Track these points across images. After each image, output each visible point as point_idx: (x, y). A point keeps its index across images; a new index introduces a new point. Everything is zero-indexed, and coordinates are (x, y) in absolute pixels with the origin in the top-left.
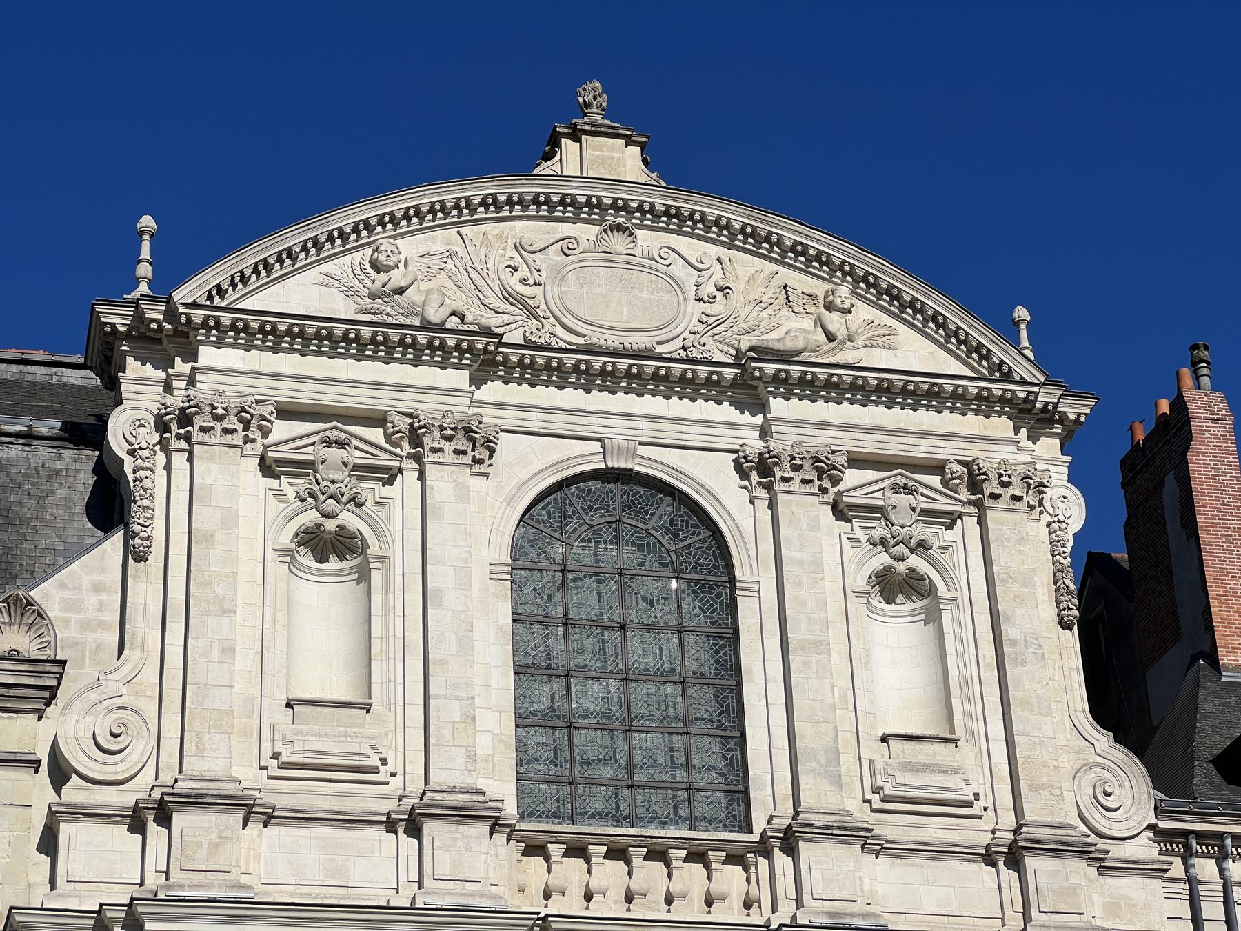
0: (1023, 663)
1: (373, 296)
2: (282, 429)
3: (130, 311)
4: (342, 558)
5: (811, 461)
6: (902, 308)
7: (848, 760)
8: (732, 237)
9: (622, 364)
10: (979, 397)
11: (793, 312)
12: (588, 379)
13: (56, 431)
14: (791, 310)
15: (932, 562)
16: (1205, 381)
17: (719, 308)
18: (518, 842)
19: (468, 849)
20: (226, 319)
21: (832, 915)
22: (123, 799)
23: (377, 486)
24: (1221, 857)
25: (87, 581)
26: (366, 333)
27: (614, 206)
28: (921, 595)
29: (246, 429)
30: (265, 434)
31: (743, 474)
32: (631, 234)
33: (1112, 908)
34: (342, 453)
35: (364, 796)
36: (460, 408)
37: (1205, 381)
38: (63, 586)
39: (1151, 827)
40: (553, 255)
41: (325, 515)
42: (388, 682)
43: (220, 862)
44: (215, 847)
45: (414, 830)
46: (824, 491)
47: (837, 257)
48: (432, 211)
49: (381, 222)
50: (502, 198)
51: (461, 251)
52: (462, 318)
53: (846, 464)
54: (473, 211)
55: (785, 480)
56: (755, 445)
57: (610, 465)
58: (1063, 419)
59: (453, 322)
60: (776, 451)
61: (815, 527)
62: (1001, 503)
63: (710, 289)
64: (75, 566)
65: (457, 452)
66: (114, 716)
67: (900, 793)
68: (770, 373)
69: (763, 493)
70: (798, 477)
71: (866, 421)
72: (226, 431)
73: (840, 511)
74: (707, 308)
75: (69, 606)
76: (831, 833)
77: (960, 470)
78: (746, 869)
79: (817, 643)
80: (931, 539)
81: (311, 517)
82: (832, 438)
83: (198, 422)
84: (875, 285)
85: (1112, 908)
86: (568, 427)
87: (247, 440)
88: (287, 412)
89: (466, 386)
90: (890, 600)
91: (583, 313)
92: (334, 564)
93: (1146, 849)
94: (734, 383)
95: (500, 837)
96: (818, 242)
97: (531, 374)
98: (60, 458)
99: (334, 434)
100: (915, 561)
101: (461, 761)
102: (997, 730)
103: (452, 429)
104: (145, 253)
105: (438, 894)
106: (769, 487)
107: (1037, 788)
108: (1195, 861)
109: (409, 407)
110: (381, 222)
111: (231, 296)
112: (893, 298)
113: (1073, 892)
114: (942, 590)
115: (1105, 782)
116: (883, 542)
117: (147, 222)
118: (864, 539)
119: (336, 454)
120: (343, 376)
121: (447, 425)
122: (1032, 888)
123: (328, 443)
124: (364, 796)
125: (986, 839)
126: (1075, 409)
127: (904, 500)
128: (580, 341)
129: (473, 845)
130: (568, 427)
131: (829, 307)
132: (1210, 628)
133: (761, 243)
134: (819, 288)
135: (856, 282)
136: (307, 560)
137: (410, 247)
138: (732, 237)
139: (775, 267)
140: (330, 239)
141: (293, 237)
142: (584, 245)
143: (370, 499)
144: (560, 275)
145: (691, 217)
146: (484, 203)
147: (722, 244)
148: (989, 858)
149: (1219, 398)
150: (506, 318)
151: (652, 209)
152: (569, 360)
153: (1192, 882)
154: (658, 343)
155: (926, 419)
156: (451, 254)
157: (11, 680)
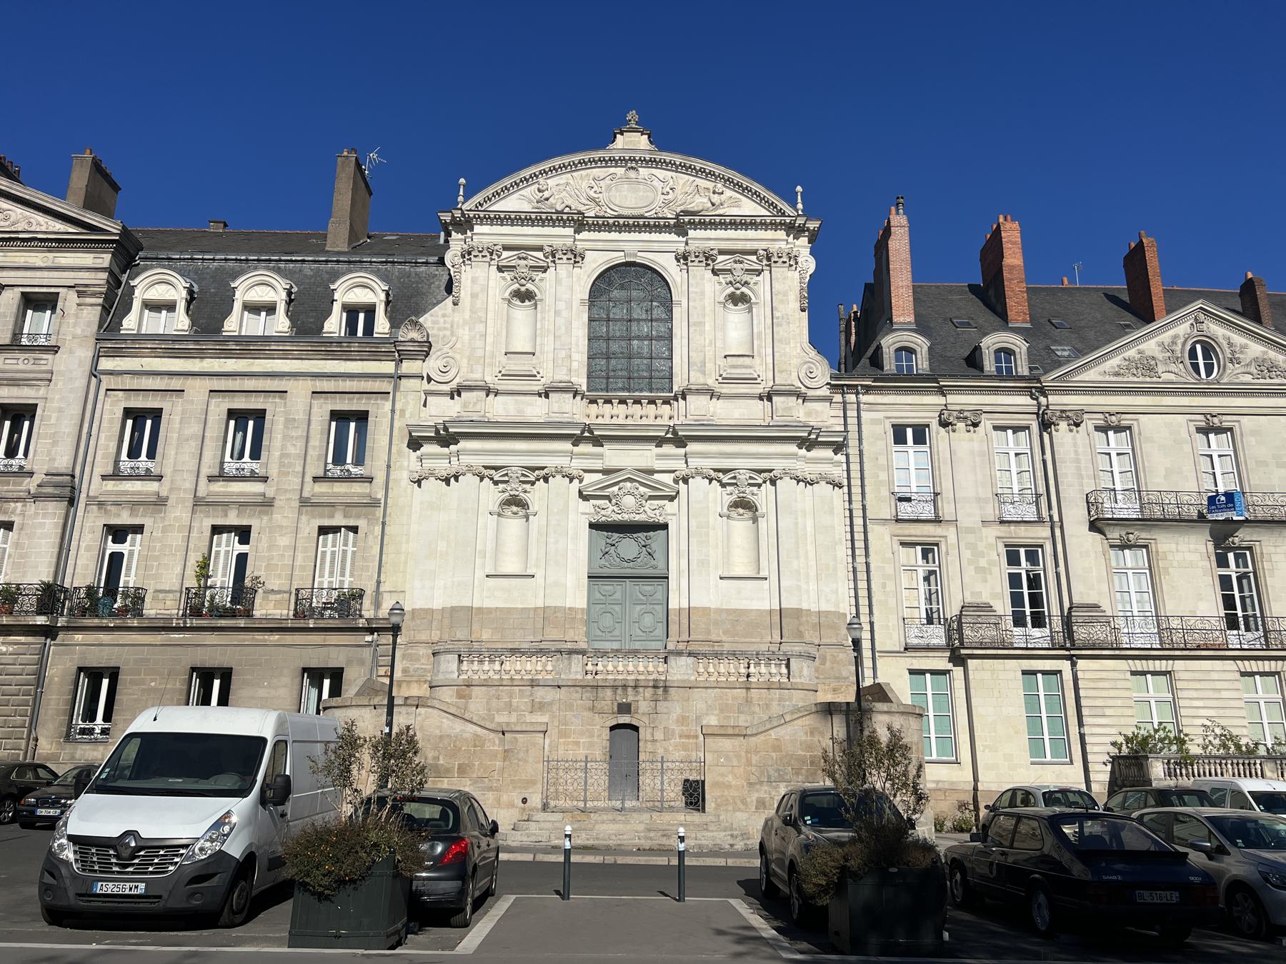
0: (781, 325)
1: (538, 202)
2: (505, 254)
3: (450, 214)
4: (530, 301)
6: (743, 190)
7: (709, 366)
8: (677, 168)
9: (631, 221)
10: (771, 223)
12: (620, 228)
13: (436, 261)
15: (750, 289)
16: (901, 211)
17: (670, 197)
19: (564, 402)
20: (482, 215)
21: (696, 421)
22: (446, 388)
24: (857, 394)
25: (440, 313)
26: (533, 216)
27: (630, 159)
28: (747, 302)
29: (575, 257)
30: (499, 257)
31: (678, 260)
33: (809, 414)
34: (525, 262)
35: (531, 385)
36: (569, 242)
37: (901, 211)
38: (432, 315)
39: (828, 384)
40: (607, 181)
42: (760, 346)
43: (477, 409)
44: (475, 404)
45: (770, 399)
46: (709, 265)
47: (717, 173)
48: (560, 167)
49: (541, 173)
50: (586, 160)
51: (572, 182)
52: (570, 208)
54: (576, 166)
55: (692, 261)
56: (681, 248)
58: (808, 230)
59: (567, 210)
61: (702, 279)
62: (778, 265)
63: (668, 189)
64: (436, 308)
65: (568, 259)
66: (445, 360)
67: (728, 376)
68: (686, 220)
69: (685, 267)
70: (697, 260)
71: (726, 237)
72: (483, 256)
73: (715, 272)
74: (666, 197)
75: (434, 322)
76: (699, 392)
77: (762, 252)
79: (700, 322)
80: (749, 280)
81: (516, 286)
82: (712, 244)
83: (473, 253)
84: (733, 182)
85: (809, 414)
87: (575, 262)
88: (506, 248)
89: (572, 234)
90: (736, 305)
91: (617, 203)
92: (527, 303)
93: (825, 392)
94: (675, 226)
95: (578, 398)
96: (710, 166)
97: (598, 227)
98: (437, 270)
99: (521, 255)
100: (744, 289)
101: (565, 371)
102: (770, 351)
104: (461, 193)
105: (778, 420)
107: (781, 372)
108: (847, 396)
109: (550, 243)
110: (541, 173)
111: (485, 206)
112: (740, 187)
113: (790, 408)
114: (754, 300)
115: (810, 368)
116: (731, 282)
117: (462, 181)
118: (724, 282)
119: (523, 262)
120: (527, 233)
122: (774, 408)
123: (520, 258)
124: (531, 385)
125: (761, 391)
126: (813, 225)
127: (738, 266)
128: (616, 214)
129: (567, 401)
131: (714, 192)
132: (891, 308)
133: (688, 169)
134: (710, 185)
135: (725, 181)
136: (731, 306)
137: (551, 182)
138: (677, 168)
140: (521, 181)
141: (507, 182)
142: (619, 176)
143: (537, 279)
144: (609, 188)
145: (660, 161)
146: (580, 162)
147: (673, 171)
148: (761, 398)
149: (905, 217)
150: (588, 207)
152: (611, 221)
153: (844, 403)
155: (751, 233)
156: (567, 184)
157: (412, 349)
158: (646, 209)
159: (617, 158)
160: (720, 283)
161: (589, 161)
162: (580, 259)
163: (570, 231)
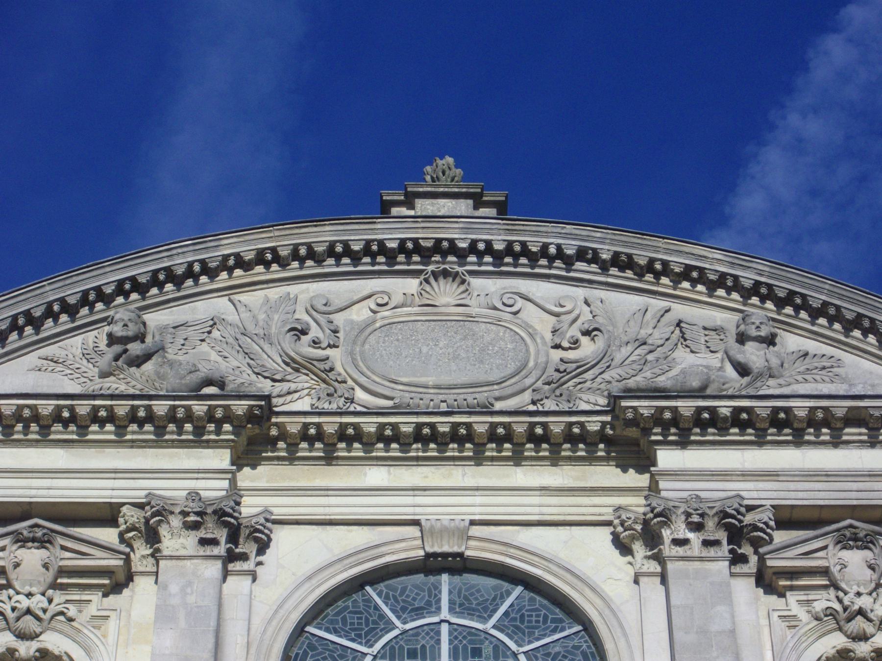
5: (716, 519)
11: (692, 352)
14: (688, 350)
23: (95, 597)
31: (624, 548)
32: (463, 282)
41: (22, 636)
50: (284, 252)
53: (772, 523)
57: (429, 549)
60: (662, 507)
63: (574, 332)
74: (571, 355)
82: (751, 491)
86: (372, 510)
103: (198, 514)
106: (659, 558)
121: (190, 510)
130: (372, 510)
139: (663, 304)
142: (397, 299)
151: (490, 248)
154: (498, 399)
158: (497, 391)
159: (393, 245)
160: (790, 620)
161: (295, 255)
162: (250, 548)
163: (221, 459)
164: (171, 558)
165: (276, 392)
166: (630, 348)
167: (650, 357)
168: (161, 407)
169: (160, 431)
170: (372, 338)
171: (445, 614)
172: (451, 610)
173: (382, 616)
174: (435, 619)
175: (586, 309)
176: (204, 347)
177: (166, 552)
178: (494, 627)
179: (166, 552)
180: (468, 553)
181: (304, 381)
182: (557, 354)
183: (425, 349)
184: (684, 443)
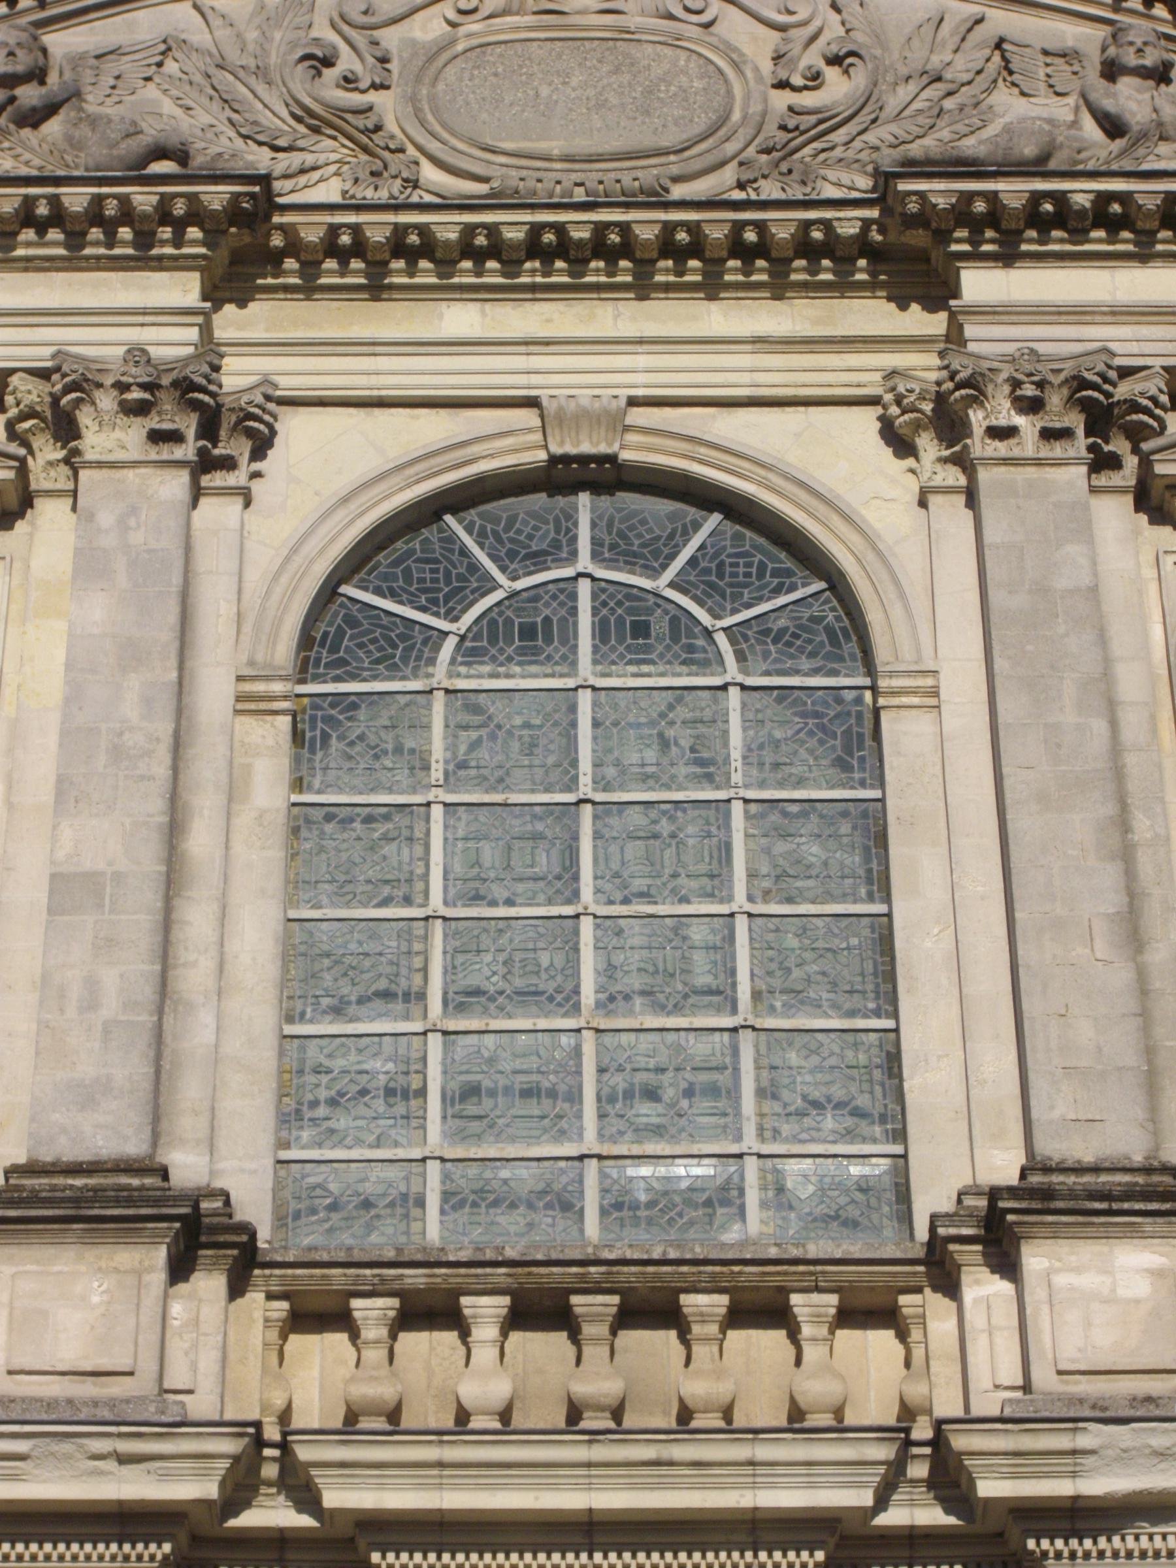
5: (1065, 392)
11: (1023, 94)
14: (1016, 91)
18: (270, 1297)
53: (1164, 399)
57: (556, 449)
60: (969, 371)
63: (813, 58)
74: (808, 100)
78: (903, 1336)
103: (144, 387)
106: (963, 461)
121: (131, 380)
154: (676, 180)
162: (240, 448)
164: (100, 465)
165: (278, 170)
166: (912, 87)
167: (949, 104)
168: (76, 199)
169: (75, 240)
170: (451, 72)
171: (584, 562)
172: (596, 556)
173: (474, 567)
174: (568, 572)
175: (834, 18)
176: (151, 92)
177: (90, 456)
178: (672, 585)
179: (90, 456)
180: (625, 455)
181: (328, 149)
182: (781, 100)
183: (545, 91)
184: (1008, 257)
